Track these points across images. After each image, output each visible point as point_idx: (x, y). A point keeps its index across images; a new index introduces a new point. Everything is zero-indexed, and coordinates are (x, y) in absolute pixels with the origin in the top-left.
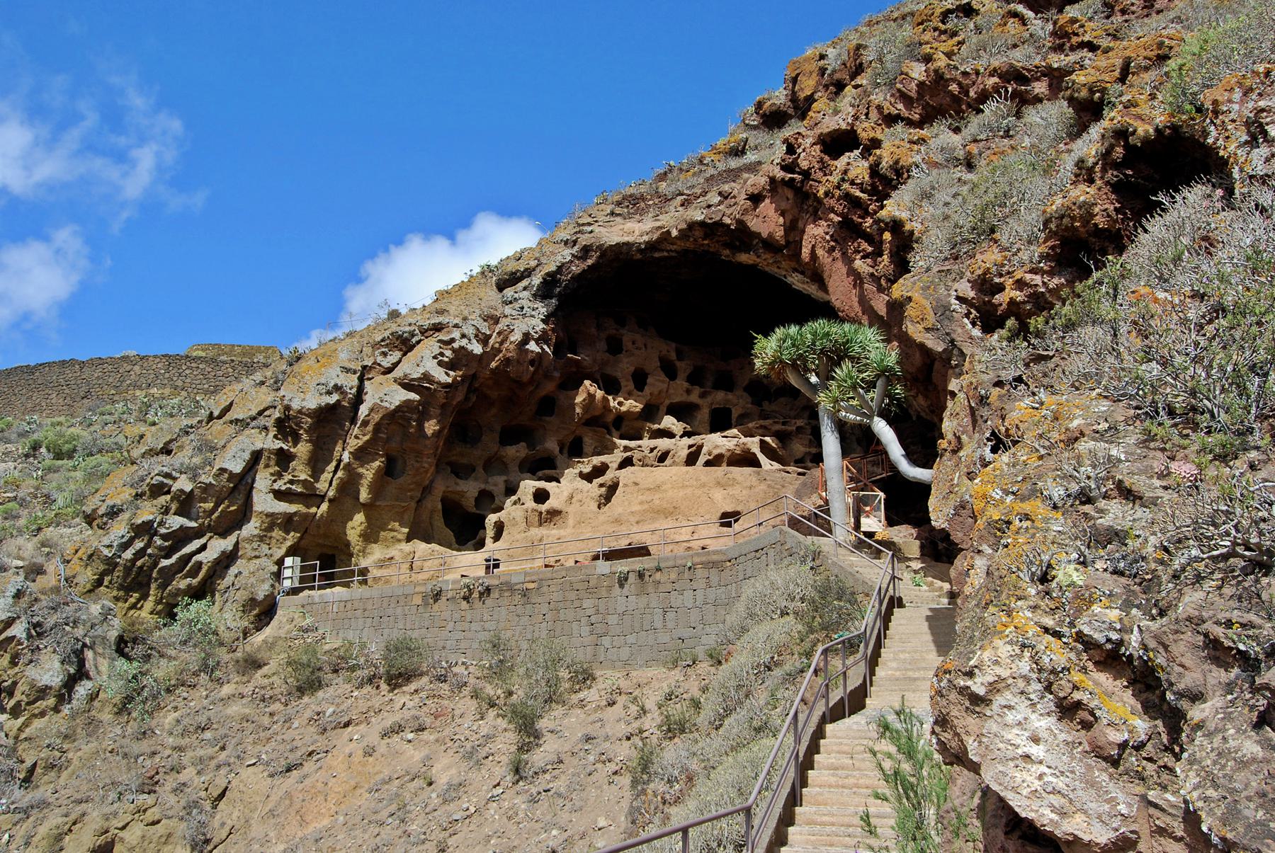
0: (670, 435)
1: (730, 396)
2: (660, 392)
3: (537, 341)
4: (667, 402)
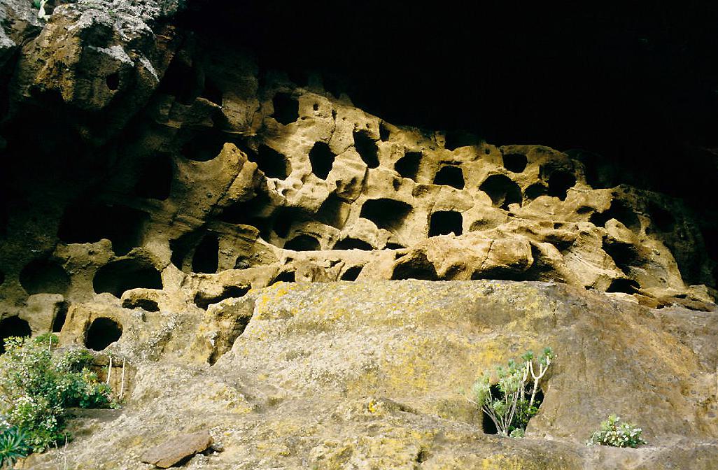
0: (366, 246)
1: (459, 194)
2: (354, 181)
3: (128, 47)
4: (363, 198)
